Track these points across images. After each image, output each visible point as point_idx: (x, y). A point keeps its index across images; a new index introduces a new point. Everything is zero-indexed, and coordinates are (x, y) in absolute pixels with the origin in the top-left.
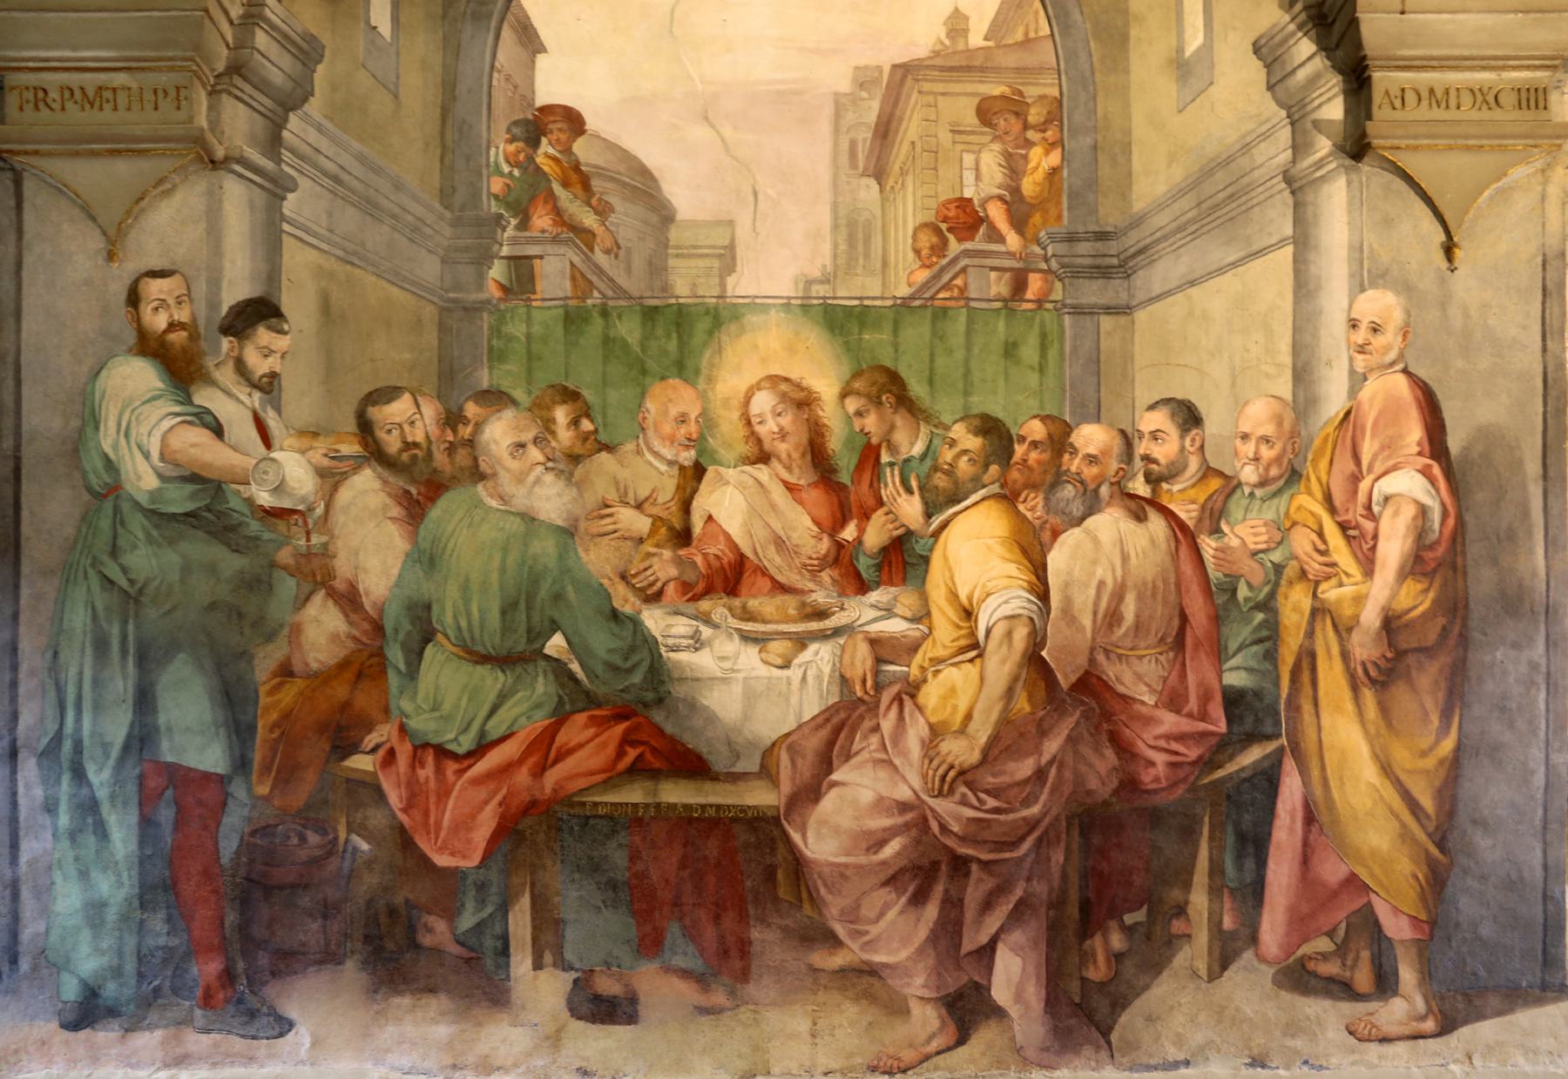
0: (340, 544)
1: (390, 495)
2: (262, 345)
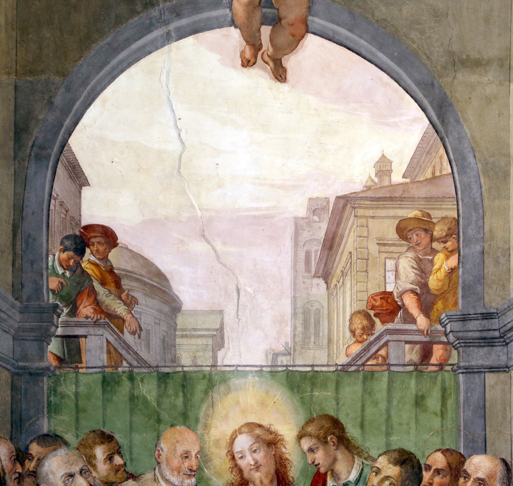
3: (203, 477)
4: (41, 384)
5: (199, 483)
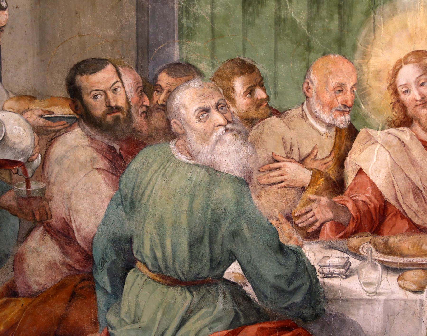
0: (55, 189)
1: (97, 150)
3: (359, 113)
4: (171, 4)
5: (354, 120)
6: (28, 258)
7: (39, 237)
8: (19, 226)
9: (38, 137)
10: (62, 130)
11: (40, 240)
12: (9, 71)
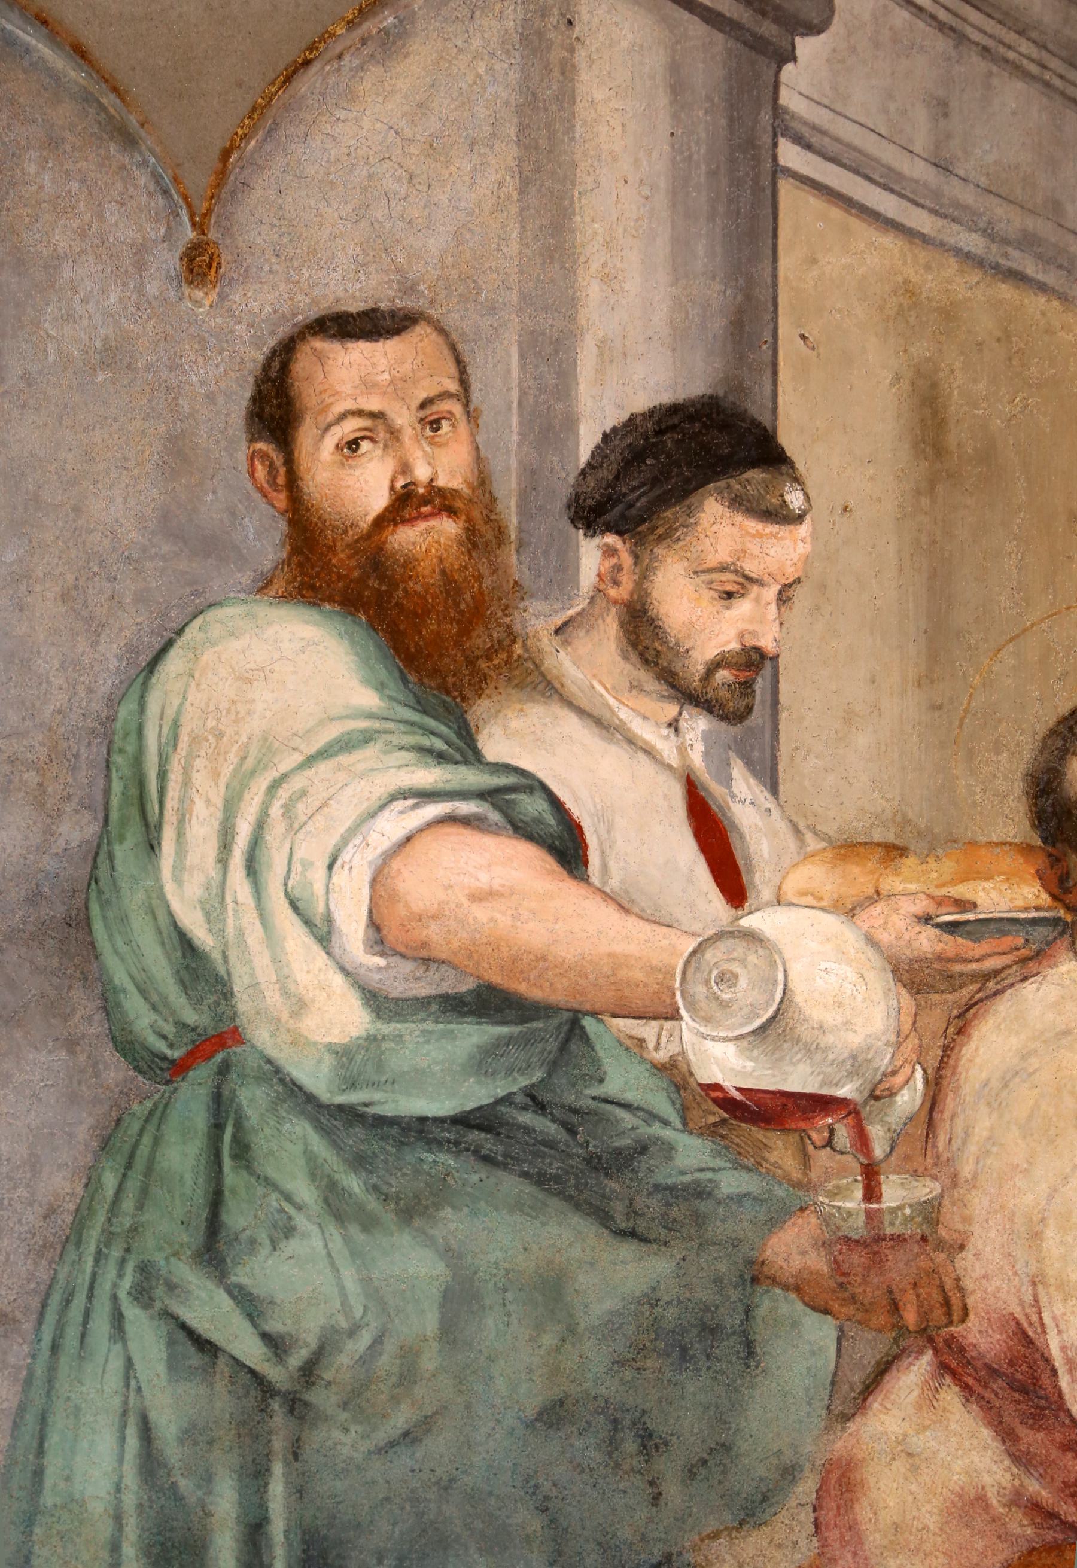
0: (979, 1203)
2: (712, 560)
6: (872, 1481)
7: (916, 1393)
8: (839, 1350)
9: (914, 1003)
10: (1007, 972)
11: (919, 1408)
12: (809, 751)
